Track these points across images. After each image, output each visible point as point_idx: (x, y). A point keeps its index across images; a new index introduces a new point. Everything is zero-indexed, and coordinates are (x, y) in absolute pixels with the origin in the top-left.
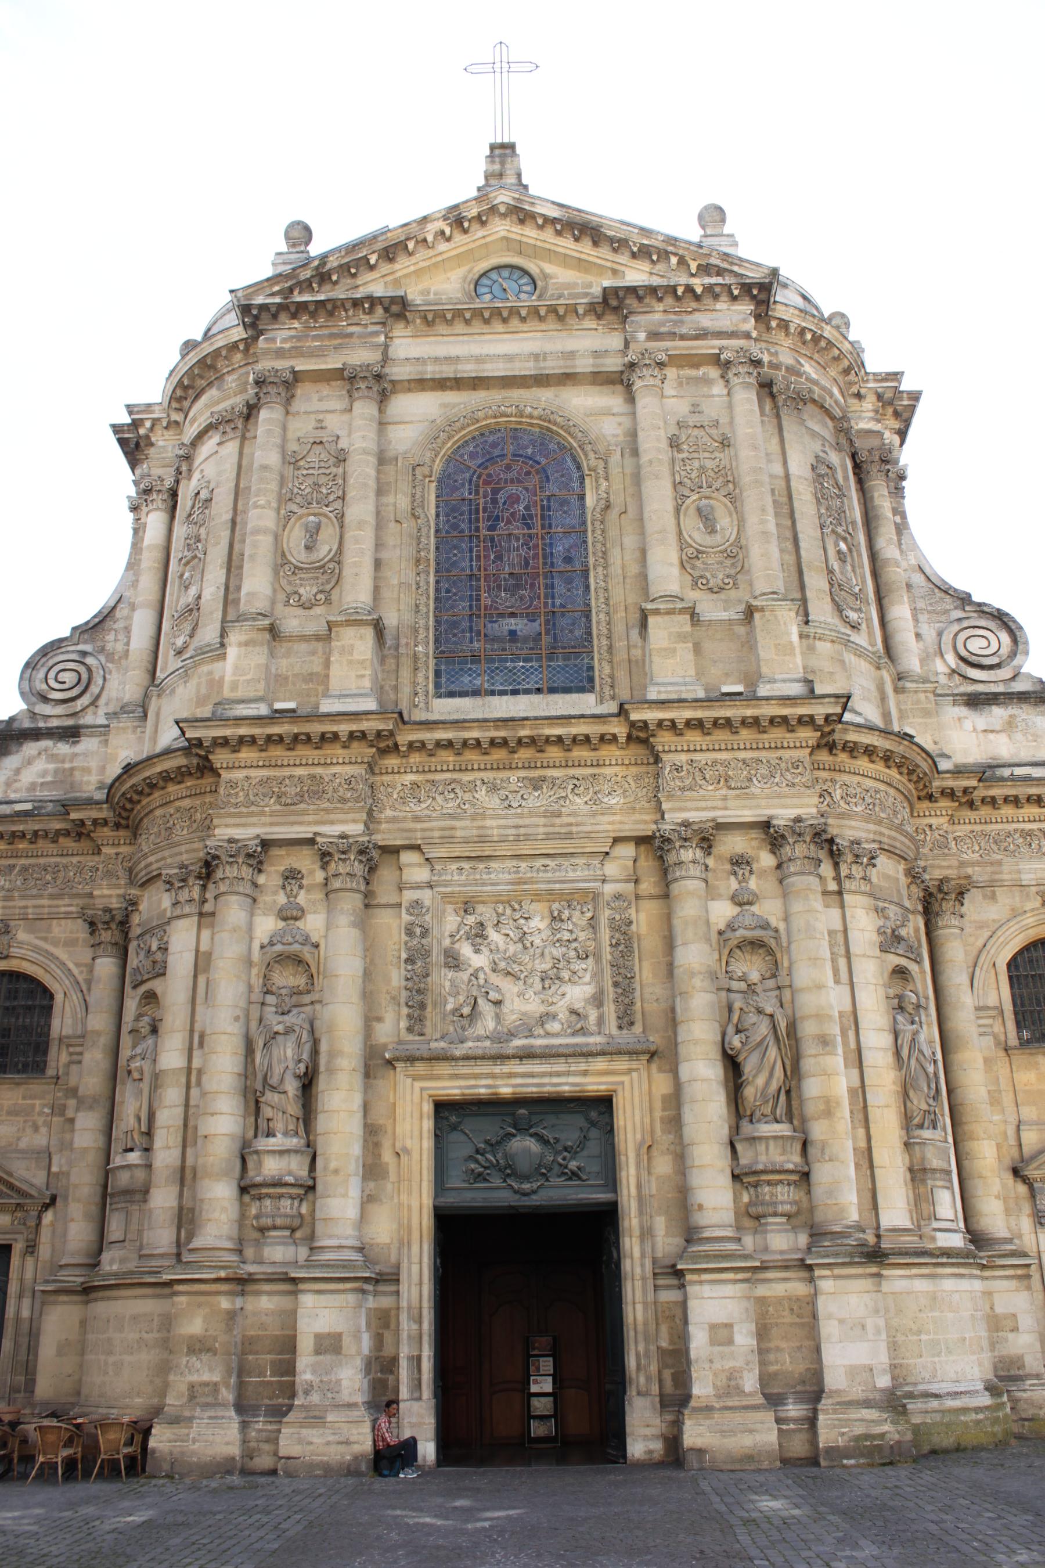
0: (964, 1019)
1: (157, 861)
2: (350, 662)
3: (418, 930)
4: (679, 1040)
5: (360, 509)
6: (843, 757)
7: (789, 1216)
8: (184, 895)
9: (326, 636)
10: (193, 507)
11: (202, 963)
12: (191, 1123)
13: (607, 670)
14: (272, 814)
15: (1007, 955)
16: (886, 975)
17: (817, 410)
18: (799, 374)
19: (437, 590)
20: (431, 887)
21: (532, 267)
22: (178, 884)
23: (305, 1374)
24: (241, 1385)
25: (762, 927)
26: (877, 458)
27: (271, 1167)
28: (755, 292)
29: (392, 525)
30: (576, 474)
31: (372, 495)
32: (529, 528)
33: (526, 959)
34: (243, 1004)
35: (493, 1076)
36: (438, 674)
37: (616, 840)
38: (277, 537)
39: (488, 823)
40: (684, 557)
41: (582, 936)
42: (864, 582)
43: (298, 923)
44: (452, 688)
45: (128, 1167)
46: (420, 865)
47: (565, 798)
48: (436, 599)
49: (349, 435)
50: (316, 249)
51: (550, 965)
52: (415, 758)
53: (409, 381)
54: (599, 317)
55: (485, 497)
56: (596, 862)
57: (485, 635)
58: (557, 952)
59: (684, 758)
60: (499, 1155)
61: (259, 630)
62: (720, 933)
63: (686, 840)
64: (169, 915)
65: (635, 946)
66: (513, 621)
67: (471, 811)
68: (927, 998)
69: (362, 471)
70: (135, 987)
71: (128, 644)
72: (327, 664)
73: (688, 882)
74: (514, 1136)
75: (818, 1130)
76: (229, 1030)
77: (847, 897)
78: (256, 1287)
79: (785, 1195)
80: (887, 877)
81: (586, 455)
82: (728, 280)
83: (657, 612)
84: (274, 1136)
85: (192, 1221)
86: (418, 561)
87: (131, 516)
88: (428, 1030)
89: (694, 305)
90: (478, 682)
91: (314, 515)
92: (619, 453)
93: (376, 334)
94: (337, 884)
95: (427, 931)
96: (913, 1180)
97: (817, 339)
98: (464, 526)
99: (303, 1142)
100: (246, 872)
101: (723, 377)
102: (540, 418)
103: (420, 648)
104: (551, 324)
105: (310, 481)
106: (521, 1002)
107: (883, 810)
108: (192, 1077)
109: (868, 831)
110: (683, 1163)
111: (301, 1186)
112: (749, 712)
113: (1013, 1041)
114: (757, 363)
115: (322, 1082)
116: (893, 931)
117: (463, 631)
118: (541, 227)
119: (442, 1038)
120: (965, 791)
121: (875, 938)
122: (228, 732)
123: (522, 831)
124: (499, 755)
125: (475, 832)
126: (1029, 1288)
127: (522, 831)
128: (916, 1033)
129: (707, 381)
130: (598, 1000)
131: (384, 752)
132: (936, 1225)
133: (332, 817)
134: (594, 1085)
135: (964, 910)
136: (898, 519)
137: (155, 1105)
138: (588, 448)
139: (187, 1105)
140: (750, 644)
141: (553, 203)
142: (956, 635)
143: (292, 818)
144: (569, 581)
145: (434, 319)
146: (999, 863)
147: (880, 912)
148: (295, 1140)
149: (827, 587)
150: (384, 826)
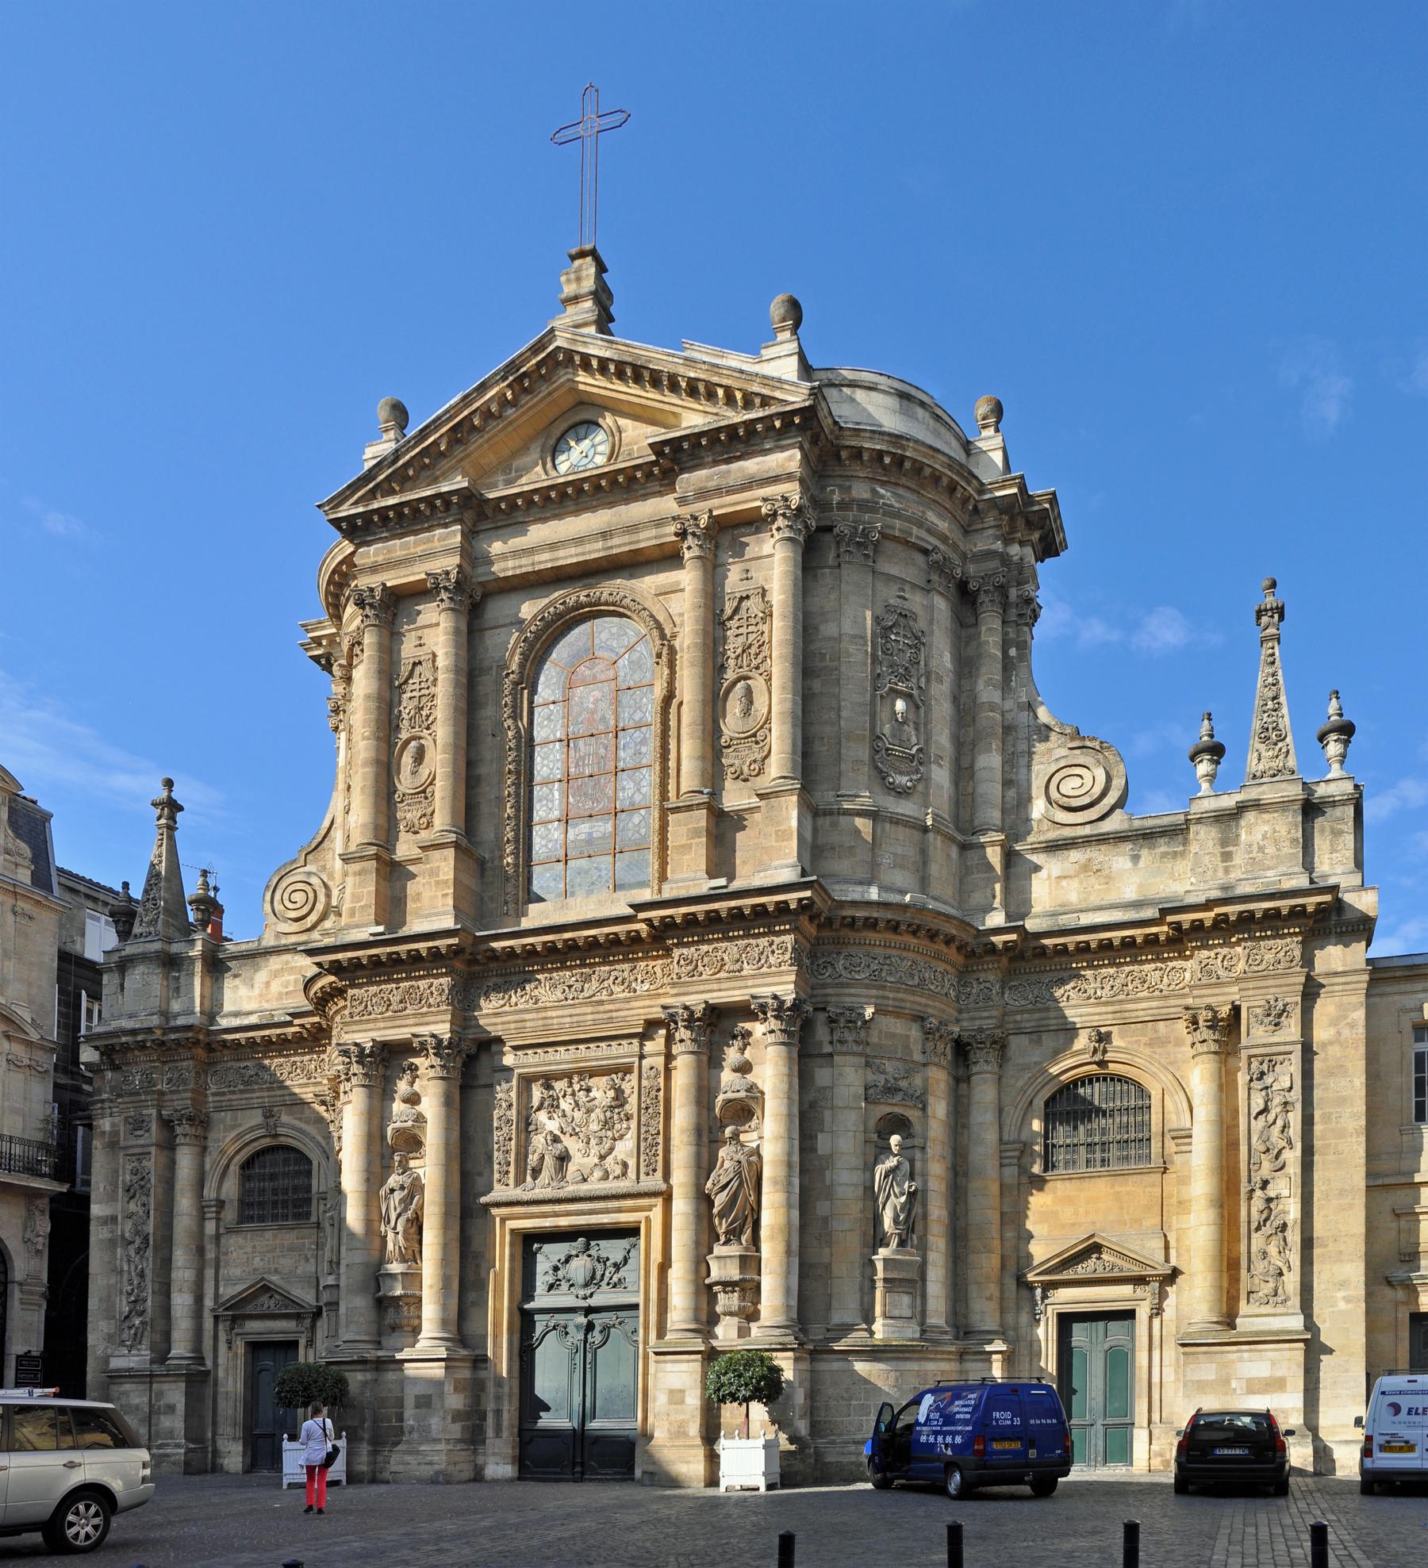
16: (872, 1124)
56: (635, 1041)
121: (861, 1091)
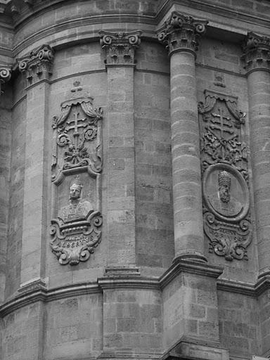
61: (209, 276)
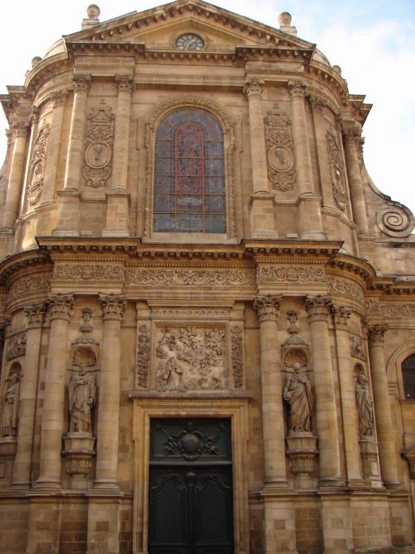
0: (384, 388)
1: (21, 302)
2: (116, 214)
3: (144, 339)
4: (263, 393)
5: (122, 143)
6: (337, 269)
7: (310, 473)
8: (34, 319)
9: (104, 202)
10: (40, 136)
11: (43, 350)
12: (37, 424)
13: (233, 223)
14: (79, 283)
15: (401, 359)
16: (353, 367)
17: (328, 111)
18: (321, 93)
19: (155, 183)
20: (151, 319)
21: (203, 36)
22: (32, 313)
23: (91, 540)
24: (61, 545)
25: (302, 344)
26: (352, 134)
27: (76, 446)
28: (305, 55)
29: (135, 150)
30: (220, 133)
31: (127, 136)
32: (198, 156)
33: (194, 354)
34: (64, 370)
35: (178, 407)
36: (154, 222)
37: (237, 302)
38: (83, 154)
39: (178, 291)
40: (270, 174)
41: (219, 344)
42: (346, 190)
43: (90, 334)
44: (163, 227)
45: (7, 443)
46: (146, 309)
47: (214, 281)
48: (155, 186)
49: (117, 107)
50: (103, 18)
51: (204, 358)
52: (145, 260)
53: (144, 84)
54: (233, 61)
55: (178, 140)
57: (177, 204)
58: (208, 351)
59: (267, 266)
60: (179, 443)
61: (74, 196)
62: (282, 346)
63: (269, 303)
64: (27, 327)
65: (243, 350)
66: (190, 198)
67: (171, 285)
68: (369, 377)
69: (122, 125)
70: (9, 360)
71: (5, 199)
72: (105, 214)
73: (270, 322)
74: (186, 434)
75: (323, 435)
76: (57, 382)
77: (338, 332)
78: (68, 500)
79: (308, 465)
80: (354, 323)
81: (225, 124)
82: (294, 48)
83: (258, 198)
84: (78, 431)
85: (38, 468)
86: (147, 168)
87: (7, 138)
88: (147, 385)
89: (276, 59)
90: (173, 226)
91: (99, 144)
92: (240, 124)
93: (131, 61)
94: (108, 316)
95: (149, 340)
96: (362, 458)
97: (330, 77)
98: (168, 153)
99: (91, 434)
100: (66, 309)
101: (289, 92)
102: (204, 105)
103: (147, 209)
104: (211, 62)
105: (97, 128)
106: (191, 374)
107: (354, 293)
108: (39, 403)
109: (347, 302)
110: (263, 448)
111: (90, 454)
112: (299, 247)
113: (403, 398)
114: (304, 87)
115: (100, 409)
116: (357, 347)
117: (167, 202)
118: (208, 17)
119: (155, 389)
120: (387, 286)
121: (349, 350)
122: (59, 244)
123: (194, 295)
124: (184, 260)
125: (172, 295)
126: (407, 506)
127: (194, 295)
128: (365, 393)
129: (282, 95)
130: (226, 374)
131: (131, 256)
132: (371, 478)
133: (107, 285)
134: (224, 412)
135: (384, 339)
136: (360, 161)
137: (20, 415)
138: (226, 121)
139: (35, 416)
140: (297, 216)
141: (214, 6)
142: (384, 215)
143: (88, 285)
144: (216, 182)
145: (157, 57)
146: (400, 319)
147: (351, 339)
148: (88, 433)
149: (332, 191)
150: (130, 291)
